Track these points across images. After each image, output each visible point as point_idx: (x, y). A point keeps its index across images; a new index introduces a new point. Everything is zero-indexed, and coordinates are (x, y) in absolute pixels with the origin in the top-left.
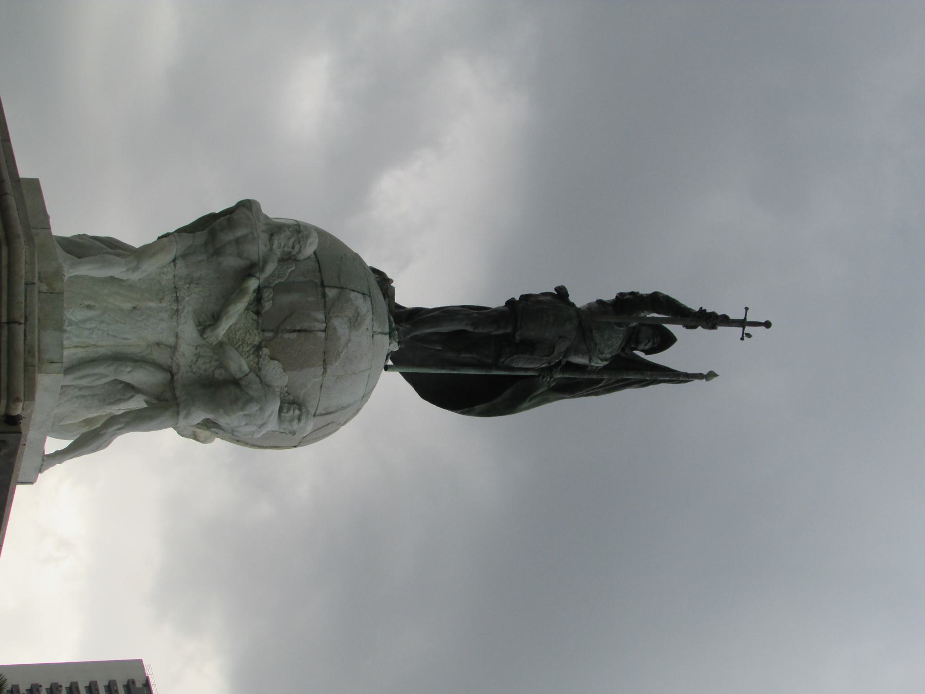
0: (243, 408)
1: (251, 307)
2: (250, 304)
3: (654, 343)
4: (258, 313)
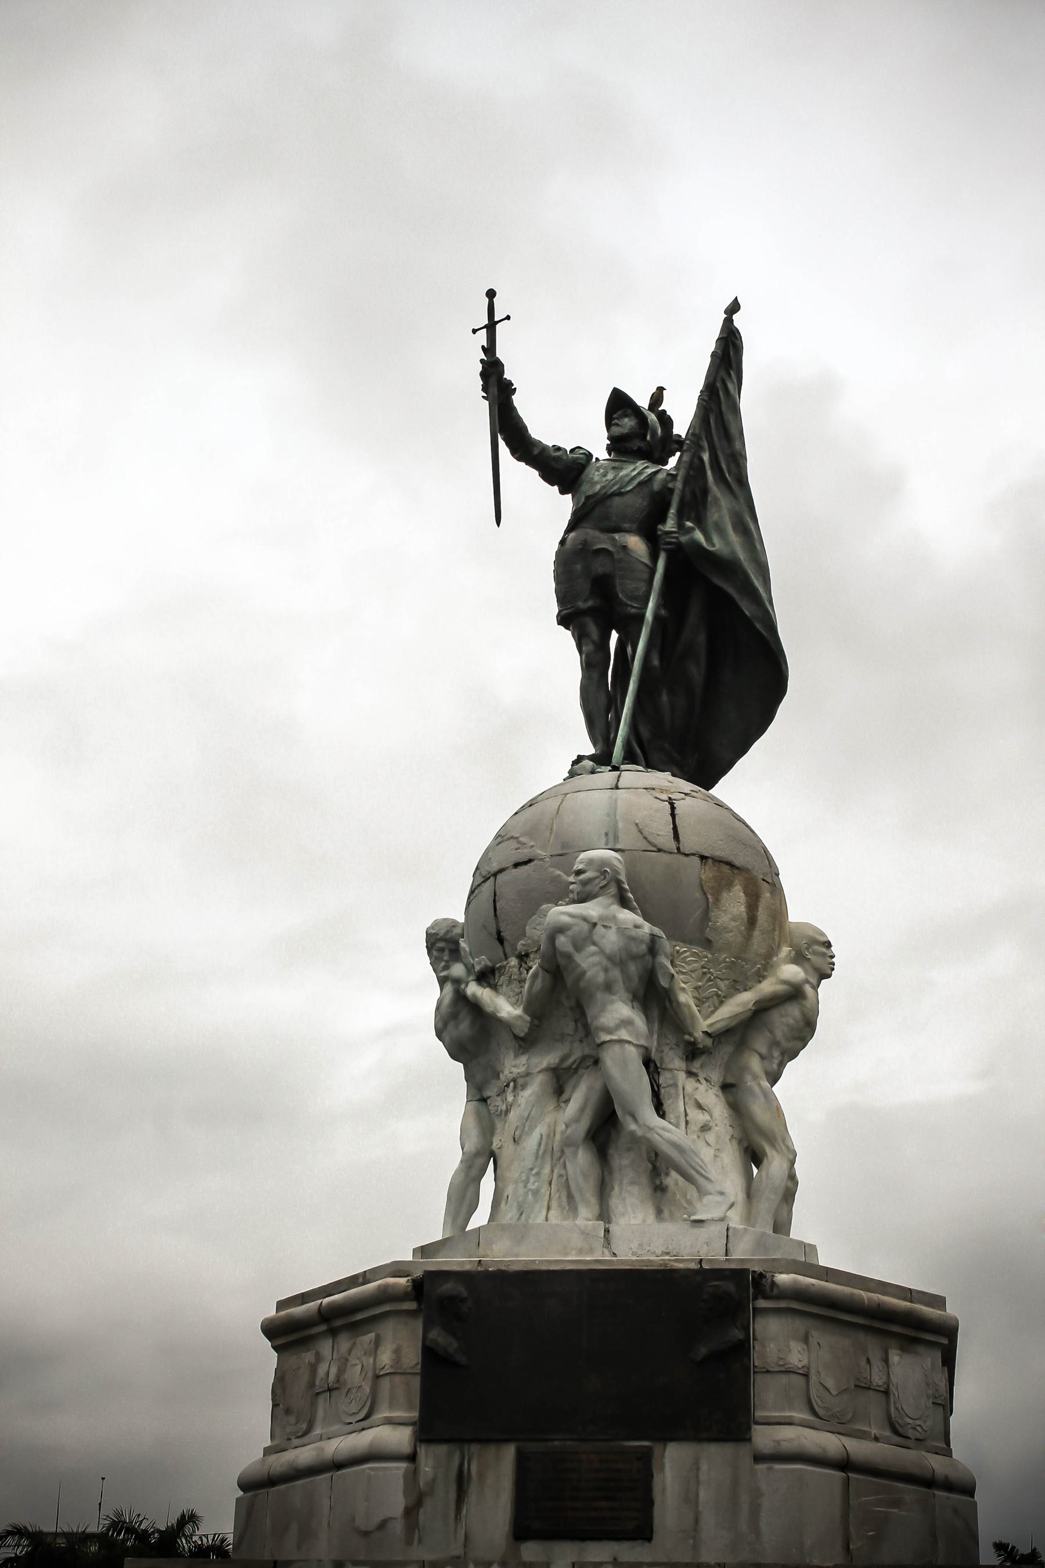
0: (569, 957)
1: (492, 982)
3: (626, 416)
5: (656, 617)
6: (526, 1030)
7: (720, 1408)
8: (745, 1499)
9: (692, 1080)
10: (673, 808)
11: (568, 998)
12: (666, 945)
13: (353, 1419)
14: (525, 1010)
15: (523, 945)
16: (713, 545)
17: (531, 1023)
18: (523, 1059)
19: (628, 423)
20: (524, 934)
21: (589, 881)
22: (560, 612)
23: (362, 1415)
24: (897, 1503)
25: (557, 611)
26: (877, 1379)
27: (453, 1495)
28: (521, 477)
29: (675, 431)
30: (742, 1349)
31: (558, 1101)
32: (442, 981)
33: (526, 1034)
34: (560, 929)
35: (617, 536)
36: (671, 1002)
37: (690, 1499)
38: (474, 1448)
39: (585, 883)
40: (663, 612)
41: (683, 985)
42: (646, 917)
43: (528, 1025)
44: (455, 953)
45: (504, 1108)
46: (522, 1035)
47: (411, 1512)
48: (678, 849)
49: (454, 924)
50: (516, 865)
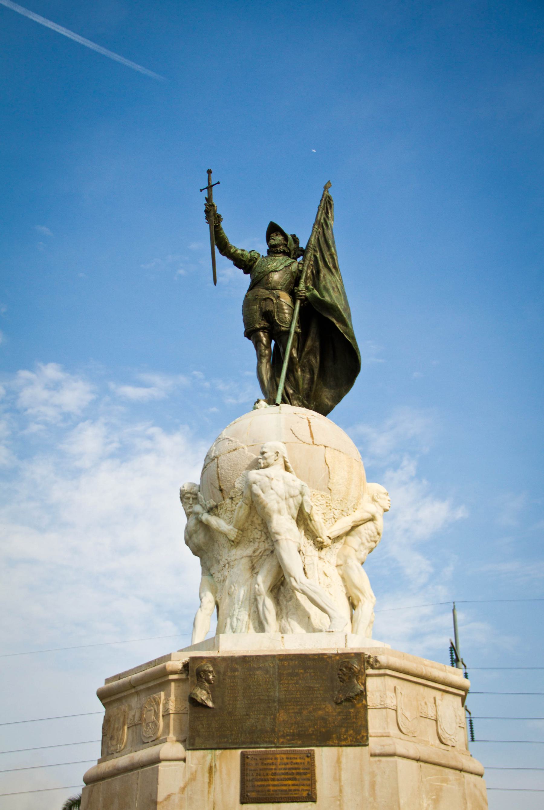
0: (257, 496)
1: (216, 513)
2: (215, 515)
3: (277, 235)
5: (296, 332)
6: (235, 536)
7: (350, 729)
8: (367, 778)
9: (321, 561)
10: (309, 423)
11: (257, 519)
12: (308, 491)
15: (234, 492)
16: (323, 297)
17: (238, 532)
19: (279, 239)
21: (269, 456)
22: (245, 330)
24: (445, 780)
25: (244, 329)
26: (431, 713)
27: (207, 780)
28: (225, 265)
29: (300, 246)
30: (363, 694)
31: (252, 573)
32: (188, 515)
33: (236, 539)
35: (274, 292)
36: (311, 520)
37: (337, 779)
38: (218, 752)
40: (299, 330)
41: (317, 512)
42: (298, 476)
43: (236, 533)
44: (196, 499)
45: (222, 578)
46: (233, 539)
48: (313, 442)
49: (195, 485)
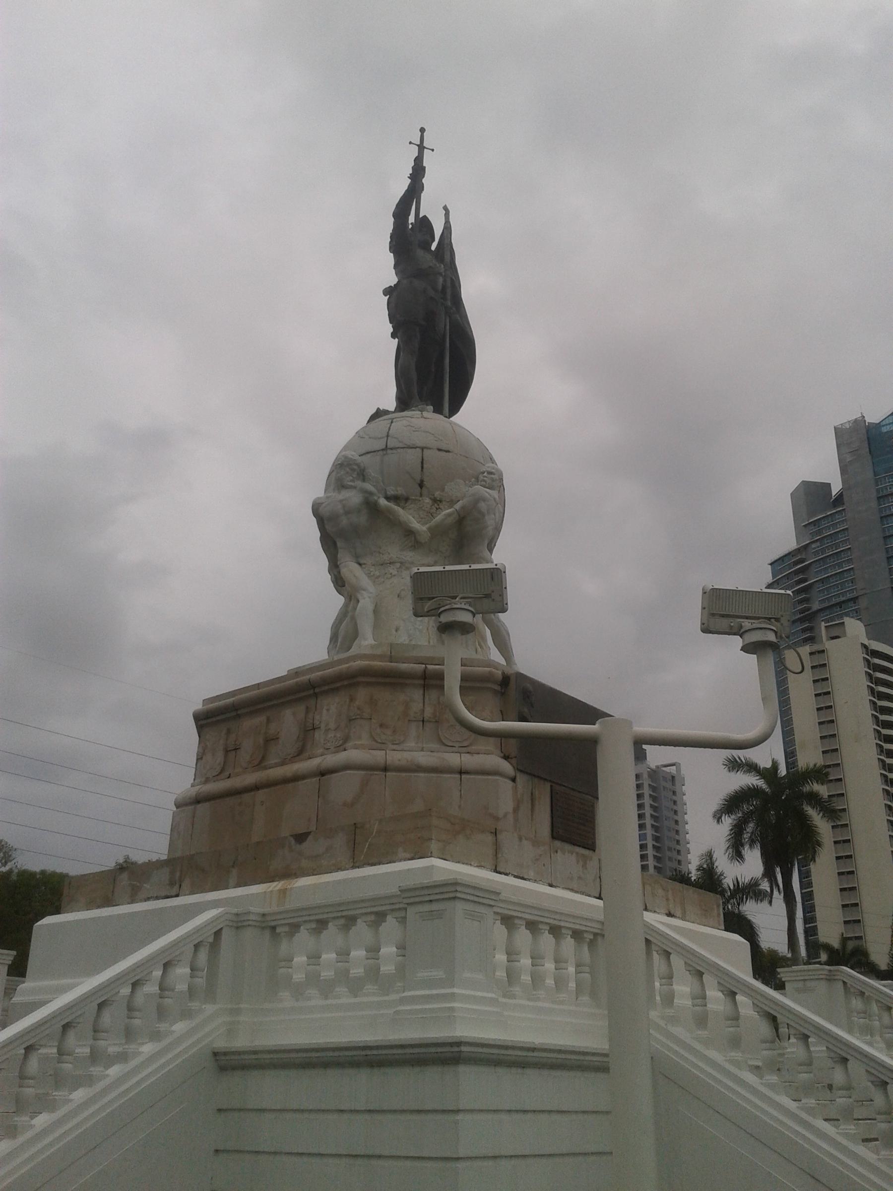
4: (407, 499)
13: (457, 745)
14: (429, 529)
18: (411, 554)
20: (443, 490)
23: (465, 744)
27: (530, 807)
34: (484, 500)
39: (493, 480)
45: (377, 573)
47: (516, 810)
50: (439, 450)
